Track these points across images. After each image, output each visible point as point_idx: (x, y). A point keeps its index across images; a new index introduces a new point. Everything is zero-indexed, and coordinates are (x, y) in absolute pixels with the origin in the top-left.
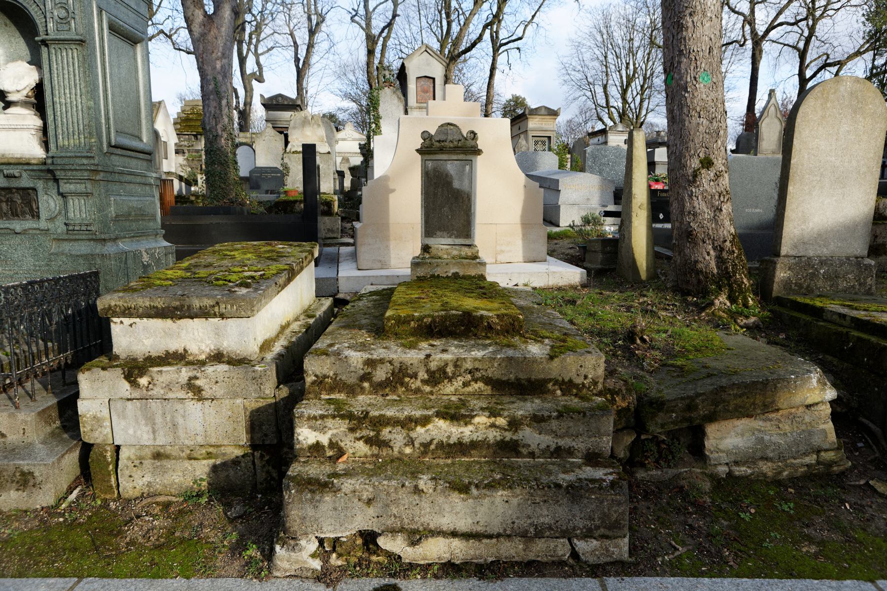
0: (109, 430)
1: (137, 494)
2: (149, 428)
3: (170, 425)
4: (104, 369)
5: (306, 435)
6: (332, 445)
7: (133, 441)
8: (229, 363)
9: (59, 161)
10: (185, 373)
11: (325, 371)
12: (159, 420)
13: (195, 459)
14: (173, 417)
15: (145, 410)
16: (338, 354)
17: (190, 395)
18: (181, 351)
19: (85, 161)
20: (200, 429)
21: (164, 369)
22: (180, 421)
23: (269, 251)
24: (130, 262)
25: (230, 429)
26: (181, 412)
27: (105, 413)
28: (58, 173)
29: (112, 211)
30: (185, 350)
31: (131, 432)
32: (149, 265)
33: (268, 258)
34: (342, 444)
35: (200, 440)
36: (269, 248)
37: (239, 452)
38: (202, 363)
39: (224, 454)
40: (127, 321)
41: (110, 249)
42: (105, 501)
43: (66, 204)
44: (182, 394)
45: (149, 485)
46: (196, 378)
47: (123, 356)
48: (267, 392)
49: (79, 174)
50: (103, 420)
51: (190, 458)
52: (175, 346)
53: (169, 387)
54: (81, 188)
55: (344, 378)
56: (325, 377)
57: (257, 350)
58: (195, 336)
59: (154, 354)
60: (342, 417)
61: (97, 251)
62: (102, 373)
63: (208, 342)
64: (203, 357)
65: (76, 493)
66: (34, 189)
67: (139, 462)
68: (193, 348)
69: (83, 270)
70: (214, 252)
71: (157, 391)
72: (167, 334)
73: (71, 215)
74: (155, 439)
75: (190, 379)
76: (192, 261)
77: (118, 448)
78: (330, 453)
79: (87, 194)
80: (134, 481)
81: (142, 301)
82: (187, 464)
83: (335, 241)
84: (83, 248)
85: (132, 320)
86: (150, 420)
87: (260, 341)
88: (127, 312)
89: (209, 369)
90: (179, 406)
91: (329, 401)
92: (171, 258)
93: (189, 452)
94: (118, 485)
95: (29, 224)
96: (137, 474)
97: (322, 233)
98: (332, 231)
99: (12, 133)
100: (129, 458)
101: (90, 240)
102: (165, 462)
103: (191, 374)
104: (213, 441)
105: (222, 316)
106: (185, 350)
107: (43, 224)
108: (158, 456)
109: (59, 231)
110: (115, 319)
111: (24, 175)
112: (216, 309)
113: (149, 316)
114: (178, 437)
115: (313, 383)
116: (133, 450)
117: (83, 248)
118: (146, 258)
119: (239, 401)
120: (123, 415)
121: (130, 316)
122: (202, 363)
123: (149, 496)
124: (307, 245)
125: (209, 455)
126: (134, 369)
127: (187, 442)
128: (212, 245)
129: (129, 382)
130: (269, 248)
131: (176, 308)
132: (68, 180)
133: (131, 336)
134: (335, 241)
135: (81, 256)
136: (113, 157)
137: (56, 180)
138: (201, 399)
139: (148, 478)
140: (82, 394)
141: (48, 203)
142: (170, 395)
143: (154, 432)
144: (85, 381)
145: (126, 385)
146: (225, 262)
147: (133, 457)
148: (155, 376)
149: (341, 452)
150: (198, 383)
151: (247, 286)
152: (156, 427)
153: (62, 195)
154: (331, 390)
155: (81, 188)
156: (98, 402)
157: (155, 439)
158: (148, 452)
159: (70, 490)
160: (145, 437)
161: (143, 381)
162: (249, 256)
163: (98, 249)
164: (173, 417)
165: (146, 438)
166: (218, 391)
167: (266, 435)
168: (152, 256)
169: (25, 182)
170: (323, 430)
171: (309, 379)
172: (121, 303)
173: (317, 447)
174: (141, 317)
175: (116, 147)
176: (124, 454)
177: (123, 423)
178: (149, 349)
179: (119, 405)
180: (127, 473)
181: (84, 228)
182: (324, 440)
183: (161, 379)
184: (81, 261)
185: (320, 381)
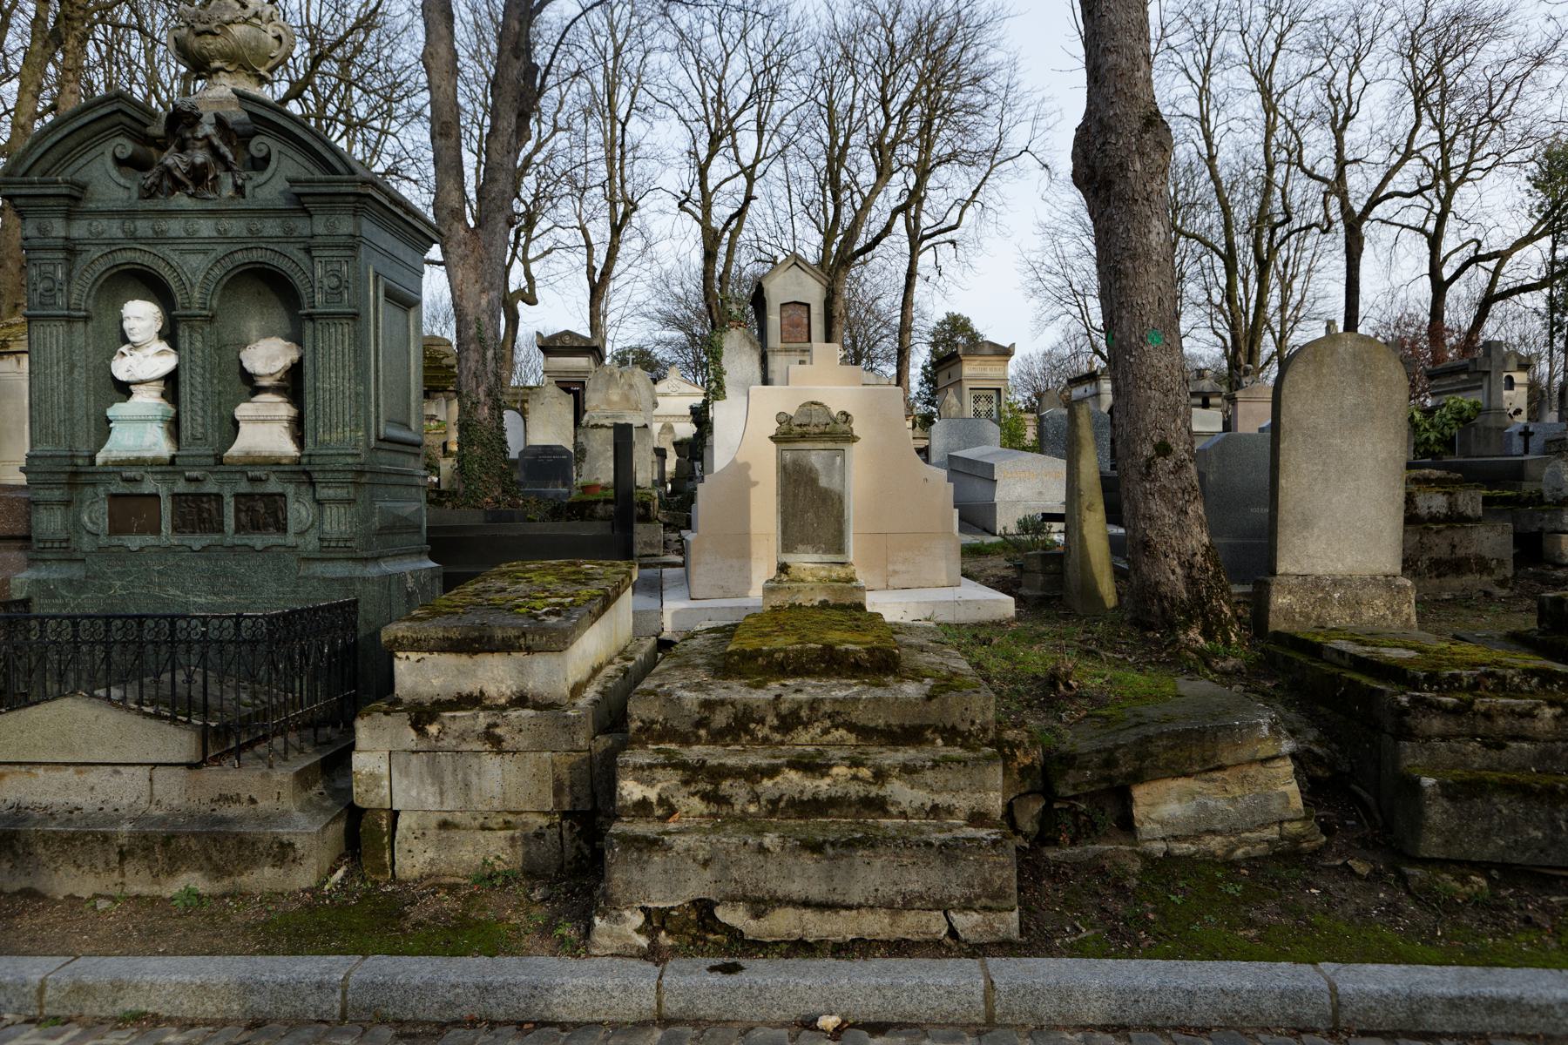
0: (387, 791)
1: (416, 873)
2: (436, 789)
3: (461, 785)
4: (387, 713)
5: (631, 790)
6: (662, 801)
7: (415, 805)
8: (537, 706)
9: (318, 460)
10: (483, 719)
11: (653, 715)
12: (448, 778)
13: (490, 829)
14: (465, 774)
16: (668, 694)
17: (488, 747)
18: (477, 693)
19: (350, 460)
20: (497, 790)
21: (458, 714)
22: (474, 779)
23: (574, 573)
24: (394, 587)
25: (535, 791)
26: (476, 767)
28: (315, 475)
29: (376, 521)
30: (481, 692)
31: (414, 793)
33: (574, 581)
34: (673, 801)
35: (496, 804)
36: (573, 569)
37: (543, 821)
38: (503, 708)
39: (525, 824)
40: (414, 656)
41: (372, 571)
42: (376, 883)
43: (321, 514)
44: (477, 746)
45: (432, 862)
46: (496, 725)
47: (406, 699)
48: (582, 743)
49: (341, 475)
51: (483, 828)
52: (469, 686)
53: (462, 737)
54: (342, 493)
55: (675, 723)
56: (653, 722)
57: (567, 693)
58: (495, 675)
59: (444, 697)
60: (675, 766)
61: (357, 573)
62: (385, 719)
63: (510, 682)
64: (503, 701)
65: (340, 873)
66: (282, 495)
68: (491, 690)
69: (339, 598)
70: (503, 574)
71: (448, 742)
72: (461, 672)
73: (327, 527)
74: (442, 803)
75: (489, 726)
76: (479, 586)
77: (395, 815)
78: (659, 812)
79: (350, 502)
80: (413, 858)
81: (433, 630)
82: (480, 835)
83: (655, 560)
84: (339, 570)
85: (420, 655)
86: (438, 779)
87: (571, 681)
88: (416, 645)
89: (513, 714)
90: (473, 761)
91: (658, 751)
92: (438, 584)
93: (481, 820)
94: (393, 863)
95: (273, 539)
96: (418, 846)
97: (638, 550)
98: (651, 545)
99: (260, 425)
100: (409, 828)
101: (348, 559)
102: (452, 833)
103: (489, 720)
104: (513, 806)
105: (529, 650)
106: (481, 692)
107: (291, 539)
108: (444, 825)
109: (310, 548)
110: (399, 654)
111: (273, 478)
112: (522, 641)
113: (442, 650)
114: (470, 801)
115: (639, 730)
116: (415, 817)
117: (339, 570)
118: (410, 584)
119: (546, 755)
120: (406, 773)
121: (419, 650)
122: (503, 708)
123: (429, 876)
124: (623, 565)
125: (507, 825)
126: (423, 714)
127: (480, 807)
128: (497, 564)
129: (416, 729)
130: (573, 569)
131: (474, 640)
132: (327, 485)
133: (416, 674)
134: (655, 560)
135: (337, 579)
136: (381, 454)
137: (312, 484)
138: (500, 752)
139: (430, 854)
140: (359, 746)
141: (299, 511)
142: (464, 747)
143: (441, 794)
144: (363, 731)
145: (413, 734)
146: (522, 586)
147: (414, 826)
148: (446, 722)
149: (672, 811)
150: (498, 731)
151: (558, 614)
152: (445, 787)
153: (319, 503)
154: (660, 738)
155: (342, 493)
156: (377, 755)
157: (442, 803)
158: (433, 820)
159: (333, 871)
160: (431, 799)
161: (433, 729)
162: (550, 578)
163: (358, 571)
164: (465, 774)
166: (522, 741)
167: (578, 799)
168: (417, 580)
169: (273, 486)
170: (650, 783)
171: (634, 725)
172: (409, 634)
173: (643, 806)
174: (431, 651)
175: (384, 440)
176: (403, 822)
177: (405, 782)
178: (438, 690)
179: (402, 758)
180: (406, 846)
181: (341, 544)
182: (652, 795)
184: (336, 586)
185: (647, 727)
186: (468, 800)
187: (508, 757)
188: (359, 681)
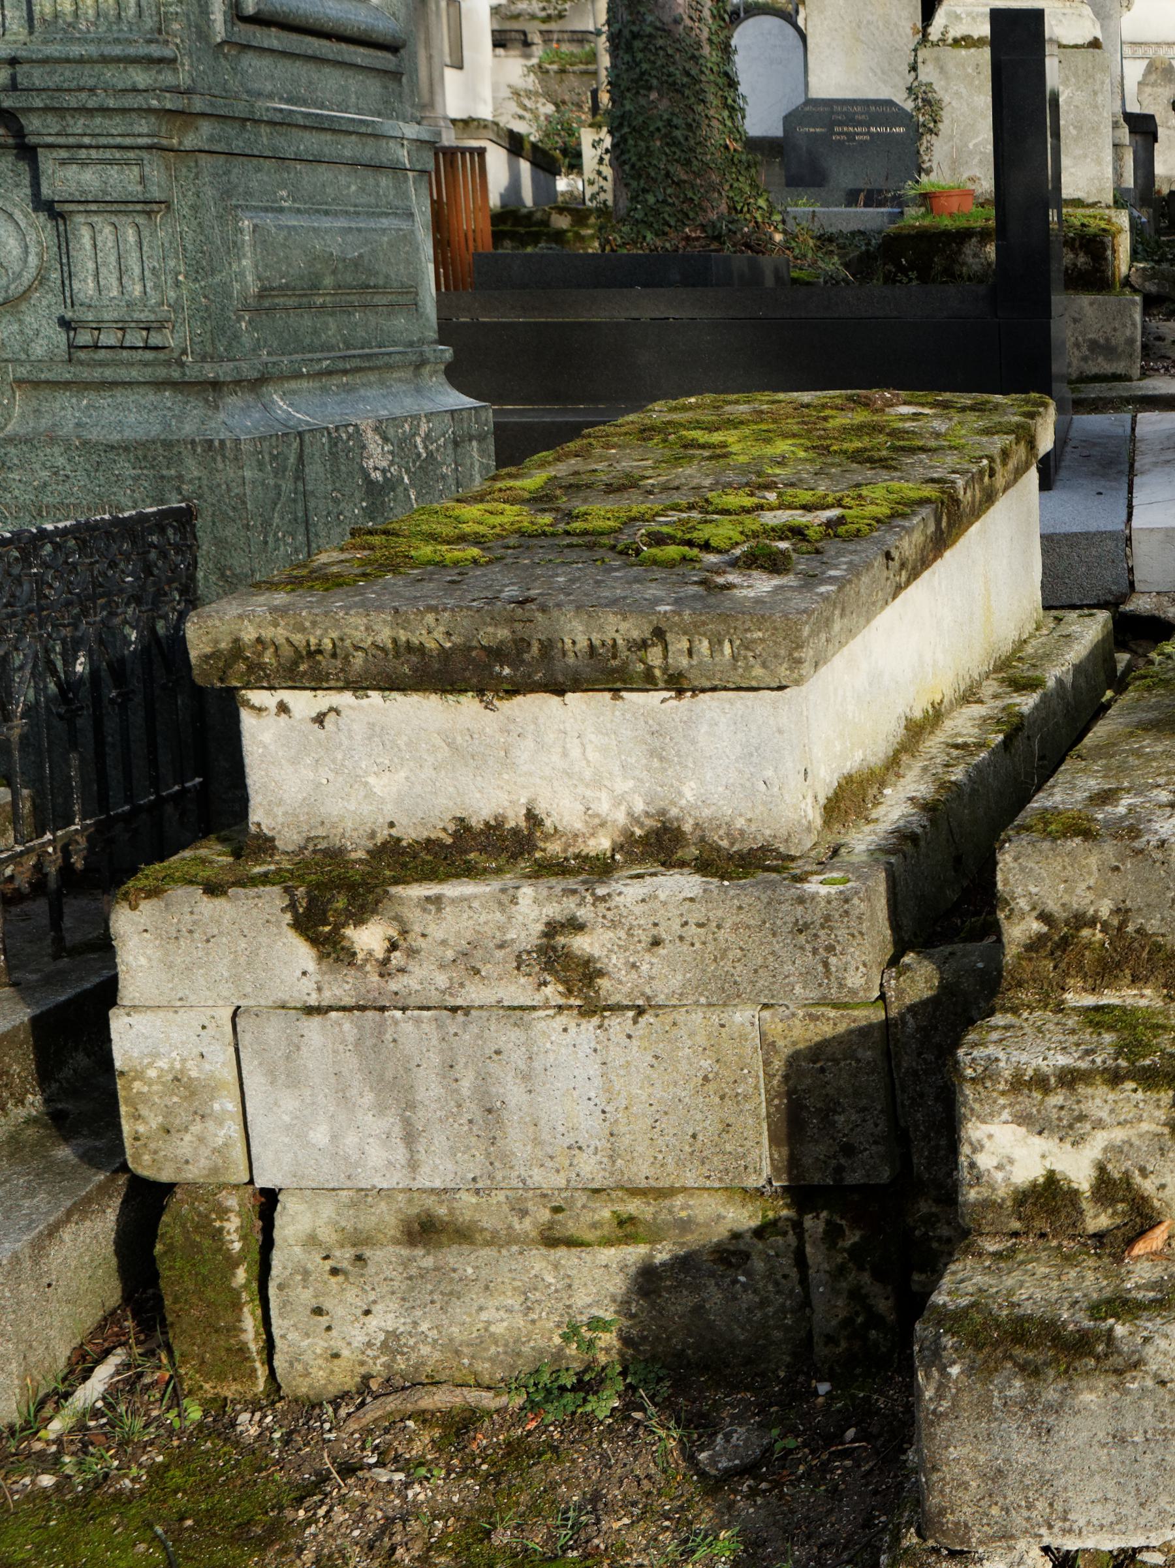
0: (233, 1129)
1: (344, 1378)
2: (390, 1122)
3: (472, 1109)
4: (213, 889)
5: (1004, 1151)
6: (1108, 1187)
7: (328, 1174)
8: (704, 866)
9: (37, 76)
10: (532, 907)
11: (1081, 898)
12: (429, 1089)
13: (571, 1243)
14: (483, 1077)
15: (373, 1049)
16: (1130, 831)
17: (553, 992)
18: (516, 819)
19: (140, 77)
20: (589, 1126)
21: (452, 890)
22: (513, 1093)
23: (859, 430)
24: (315, 470)
25: (709, 1127)
26: (517, 1058)
27: (220, 1062)
28: (33, 124)
29: (246, 272)
30: (531, 816)
31: (320, 1135)
32: (391, 484)
33: (858, 457)
34: (1148, 1186)
35: (590, 1168)
36: (861, 416)
37: (742, 1217)
38: (600, 869)
39: (685, 1225)
40: (304, 703)
41: (237, 419)
42: (219, 1407)
43: (64, 244)
44: (518, 991)
45: (391, 1343)
46: (576, 926)
47: (288, 840)
48: (855, 980)
49: (115, 125)
50: (212, 1089)
51: (551, 1240)
52: (491, 799)
53: (467, 962)
54: (123, 180)
55: (1153, 925)
56: (1081, 920)
57: (814, 816)
58: (573, 762)
59: (409, 832)
60: (1149, 1079)
61: (189, 429)
62: (208, 906)
63: (623, 785)
64: (602, 844)
65: (103, 1374)
67: (352, 1256)
68: (564, 810)
69: (133, 502)
70: (645, 432)
71: (423, 978)
72: (461, 752)
73: (85, 287)
74: (413, 1165)
75: (552, 929)
76: (561, 469)
77: (268, 1202)
78: (1098, 1220)
79: (149, 207)
80: (330, 1330)
81: (365, 626)
82: (539, 1262)
83: (1120, 389)
84: (132, 417)
85: (325, 700)
86: (396, 1092)
87: (826, 779)
88: (306, 669)
89: (628, 892)
90: (507, 1036)
91: (1097, 1018)
92: (479, 457)
93: (545, 1215)
94: (270, 1346)
96: (344, 1301)
97: (1069, 358)
98: (1105, 349)
100: (312, 1241)
101: (158, 385)
102: (457, 1259)
103: (554, 910)
104: (641, 1172)
105: (678, 684)
106: (531, 816)
108: (425, 1231)
109: (39, 350)
110: (257, 697)
112: (654, 656)
113: (392, 684)
114: (506, 1159)
115: (1035, 945)
116: (327, 1210)
117: (132, 417)
118: (378, 457)
119: (742, 1016)
120: (288, 1074)
121: (317, 682)
122: (600, 869)
123: (391, 1387)
124: (1008, 406)
125: (626, 1229)
126: (333, 892)
127: (538, 1177)
128: (639, 402)
129: (315, 941)
130: (861, 416)
131: (497, 653)
132: (74, 154)
133: (321, 763)
134: (1120, 389)
135: (125, 448)
136: (250, 61)
137: (27, 152)
138: (590, 1010)
139: (385, 1319)
140: (129, 991)
142: (474, 993)
143: (410, 1137)
144: (146, 940)
145: (303, 954)
146: (691, 473)
147: (327, 1235)
148: (417, 919)
149: (1142, 1217)
150: (582, 944)
151: (775, 564)
152: (419, 1118)
153: (52, 210)
154: (1105, 972)
155: (123, 180)
156: (192, 1019)
157: (413, 1165)
158: (385, 1217)
159: (82, 1366)
160: (376, 1155)
161: (368, 938)
162: (782, 446)
163: (193, 420)
164: (483, 1077)
165: (377, 1159)
166: (663, 975)
167: (848, 1150)
168: (402, 447)
170: (1071, 1129)
171: (1019, 930)
172: (279, 633)
173: (1048, 1198)
174: (358, 686)
175: (259, 20)
176: (290, 1224)
177: (289, 1103)
178: (390, 812)
179: (274, 1029)
180: (305, 1297)
181: (135, 338)
182: (1078, 1167)
183: (437, 932)
184: (125, 467)
185: (1061, 940)
186: (497, 1156)
187: (618, 1024)
188: (159, 780)
